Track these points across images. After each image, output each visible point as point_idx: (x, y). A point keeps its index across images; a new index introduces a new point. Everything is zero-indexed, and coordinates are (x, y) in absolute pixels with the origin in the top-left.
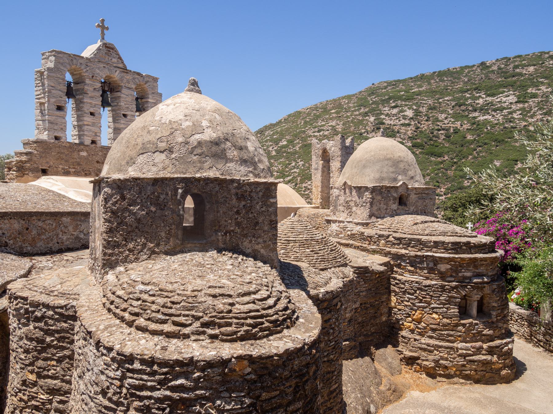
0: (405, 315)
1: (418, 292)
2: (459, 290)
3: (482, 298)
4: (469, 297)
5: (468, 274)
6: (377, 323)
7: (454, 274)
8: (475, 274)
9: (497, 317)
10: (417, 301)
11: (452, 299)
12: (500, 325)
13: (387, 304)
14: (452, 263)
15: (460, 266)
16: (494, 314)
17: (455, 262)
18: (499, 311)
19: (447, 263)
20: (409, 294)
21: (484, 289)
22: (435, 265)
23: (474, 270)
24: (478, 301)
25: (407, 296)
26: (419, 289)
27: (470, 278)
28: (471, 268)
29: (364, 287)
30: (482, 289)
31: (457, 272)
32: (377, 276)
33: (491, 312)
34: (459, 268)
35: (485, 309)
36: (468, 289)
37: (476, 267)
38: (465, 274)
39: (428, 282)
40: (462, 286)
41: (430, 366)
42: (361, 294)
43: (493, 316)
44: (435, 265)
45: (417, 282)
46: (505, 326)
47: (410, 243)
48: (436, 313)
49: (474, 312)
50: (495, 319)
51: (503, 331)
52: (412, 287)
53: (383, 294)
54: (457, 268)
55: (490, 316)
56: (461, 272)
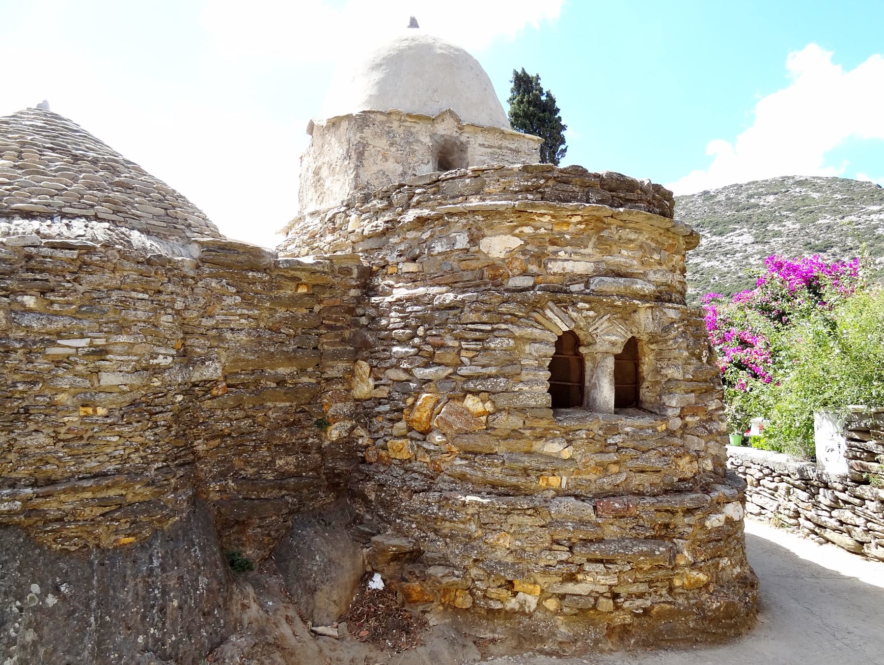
0: (388, 416)
1: (421, 331)
2: (549, 313)
3: (632, 345)
4: (589, 344)
5: (581, 267)
6: (306, 447)
7: (533, 268)
8: (603, 266)
9: (681, 417)
10: (419, 360)
11: (527, 348)
12: (695, 443)
13: (348, 391)
14: (528, 230)
15: (553, 243)
16: (674, 403)
17: (536, 229)
18: (692, 398)
19: (511, 231)
20: (400, 343)
21: (636, 316)
22: (474, 240)
23: (598, 256)
24: (617, 357)
25: (395, 349)
26: (423, 320)
27: (586, 279)
28: (588, 251)
29: (241, 316)
30: (626, 314)
31: (540, 258)
32: (303, 290)
33: (665, 399)
34: (551, 248)
35: (646, 394)
36: (580, 311)
37: (604, 245)
38: (569, 266)
39: (450, 297)
40: (557, 302)
41: (445, 581)
42: (229, 335)
43: (670, 412)
44: (474, 240)
45: (415, 300)
46: (713, 449)
47: (411, 198)
48: (476, 393)
49: (605, 392)
50: (679, 422)
51: (709, 465)
52: (407, 317)
53: (336, 356)
54: (541, 246)
55: (658, 411)
56: (555, 260)
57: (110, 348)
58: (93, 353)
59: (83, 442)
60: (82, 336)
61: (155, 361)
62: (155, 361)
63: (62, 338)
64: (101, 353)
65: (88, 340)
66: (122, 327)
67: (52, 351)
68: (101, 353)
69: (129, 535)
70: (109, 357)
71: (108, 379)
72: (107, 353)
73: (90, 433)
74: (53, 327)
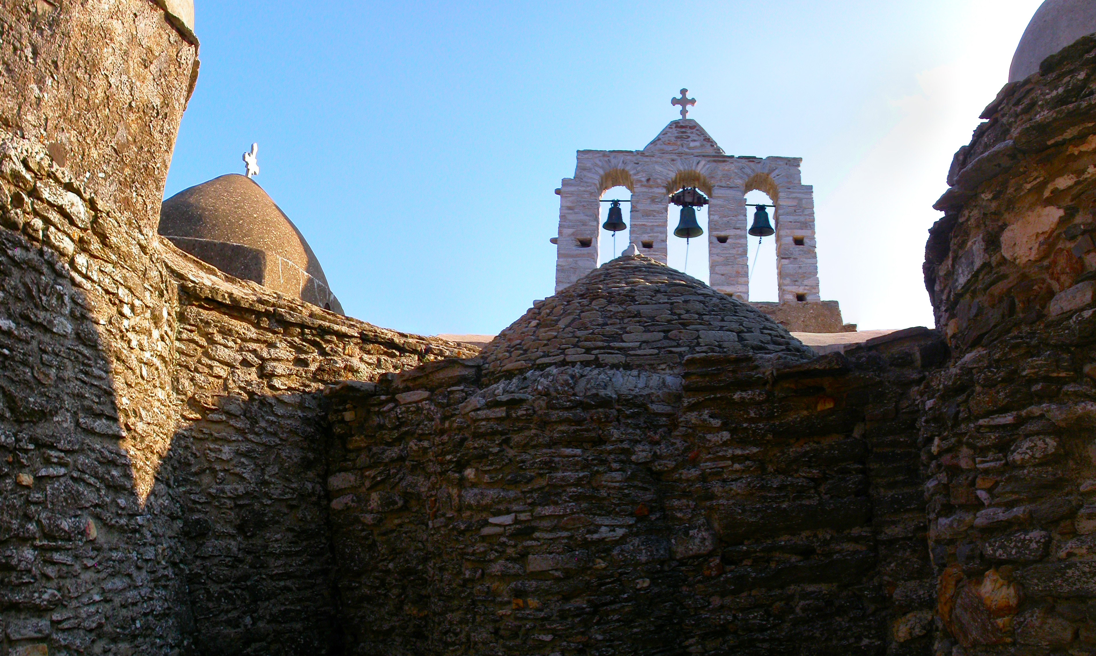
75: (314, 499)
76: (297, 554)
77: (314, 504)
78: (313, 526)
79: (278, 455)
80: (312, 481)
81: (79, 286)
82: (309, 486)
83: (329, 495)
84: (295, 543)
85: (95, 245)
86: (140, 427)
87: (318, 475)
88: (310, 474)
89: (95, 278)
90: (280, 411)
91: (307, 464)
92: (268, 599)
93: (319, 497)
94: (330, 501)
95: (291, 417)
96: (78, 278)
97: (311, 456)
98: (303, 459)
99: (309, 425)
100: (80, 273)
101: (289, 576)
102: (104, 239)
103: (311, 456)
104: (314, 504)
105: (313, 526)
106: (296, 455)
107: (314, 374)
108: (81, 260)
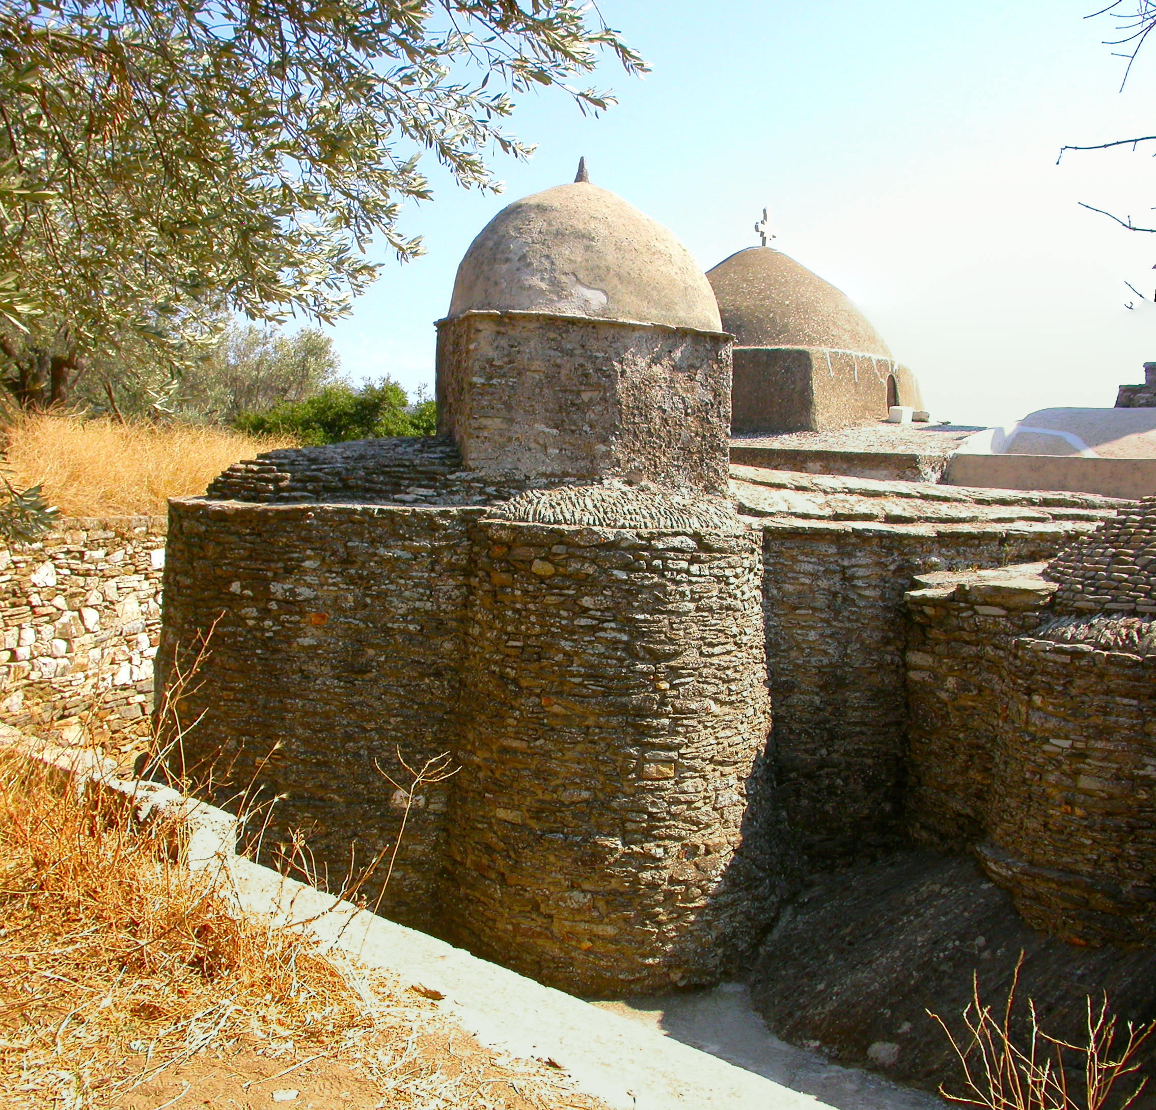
57: (1087, 752)
58: (1073, 755)
59: (1063, 837)
60: (1067, 738)
61: (1141, 772)
62: (1141, 772)
63: (1055, 737)
64: (1081, 755)
65: (1070, 742)
66: (1103, 733)
67: (1047, 747)
68: (1081, 755)
69: (1080, 937)
70: (1088, 761)
71: (1085, 782)
72: (1087, 757)
73: (1068, 830)
74: (1049, 725)
75: (893, 667)
76: (874, 708)
77: (892, 672)
78: (891, 688)
79: (859, 636)
80: (892, 654)
81: (697, 582)
82: (888, 658)
83: (906, 666)
84: (873, 700)
85: (703, 556)
86: (745, 639)
87: (898, 649)
88: (890, 648)
89: (707, 572)
90: (862, 604)
91: (887, 641)
92: (844, 739)
93: (898, 666)
94: (907, 670)
95: (872, 606)
96: (694, 579)
97: (891, 635)
98: (883, 637)
99: (890, 612)
100: (695, 576)
101: (865, 724)
102: (708, 549)
103: (891, 635)
104: (892, 672)
105: (891, 688)
106: (877, 636)
107: (894, 572)
108: (694, 569)
